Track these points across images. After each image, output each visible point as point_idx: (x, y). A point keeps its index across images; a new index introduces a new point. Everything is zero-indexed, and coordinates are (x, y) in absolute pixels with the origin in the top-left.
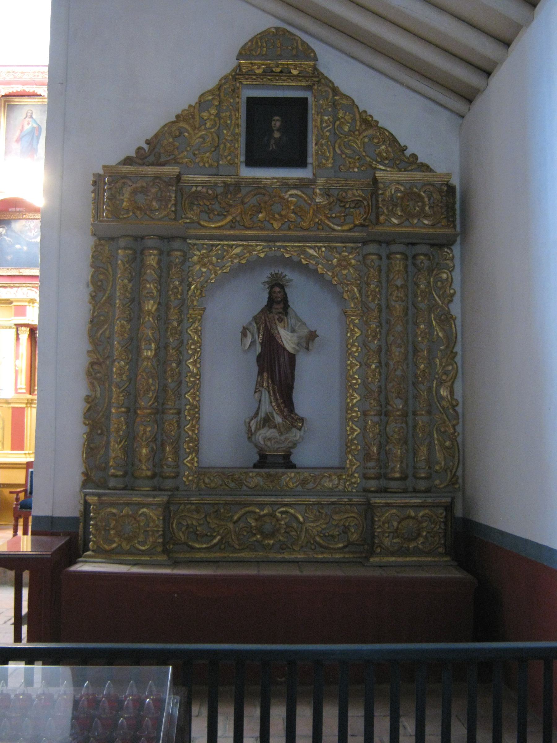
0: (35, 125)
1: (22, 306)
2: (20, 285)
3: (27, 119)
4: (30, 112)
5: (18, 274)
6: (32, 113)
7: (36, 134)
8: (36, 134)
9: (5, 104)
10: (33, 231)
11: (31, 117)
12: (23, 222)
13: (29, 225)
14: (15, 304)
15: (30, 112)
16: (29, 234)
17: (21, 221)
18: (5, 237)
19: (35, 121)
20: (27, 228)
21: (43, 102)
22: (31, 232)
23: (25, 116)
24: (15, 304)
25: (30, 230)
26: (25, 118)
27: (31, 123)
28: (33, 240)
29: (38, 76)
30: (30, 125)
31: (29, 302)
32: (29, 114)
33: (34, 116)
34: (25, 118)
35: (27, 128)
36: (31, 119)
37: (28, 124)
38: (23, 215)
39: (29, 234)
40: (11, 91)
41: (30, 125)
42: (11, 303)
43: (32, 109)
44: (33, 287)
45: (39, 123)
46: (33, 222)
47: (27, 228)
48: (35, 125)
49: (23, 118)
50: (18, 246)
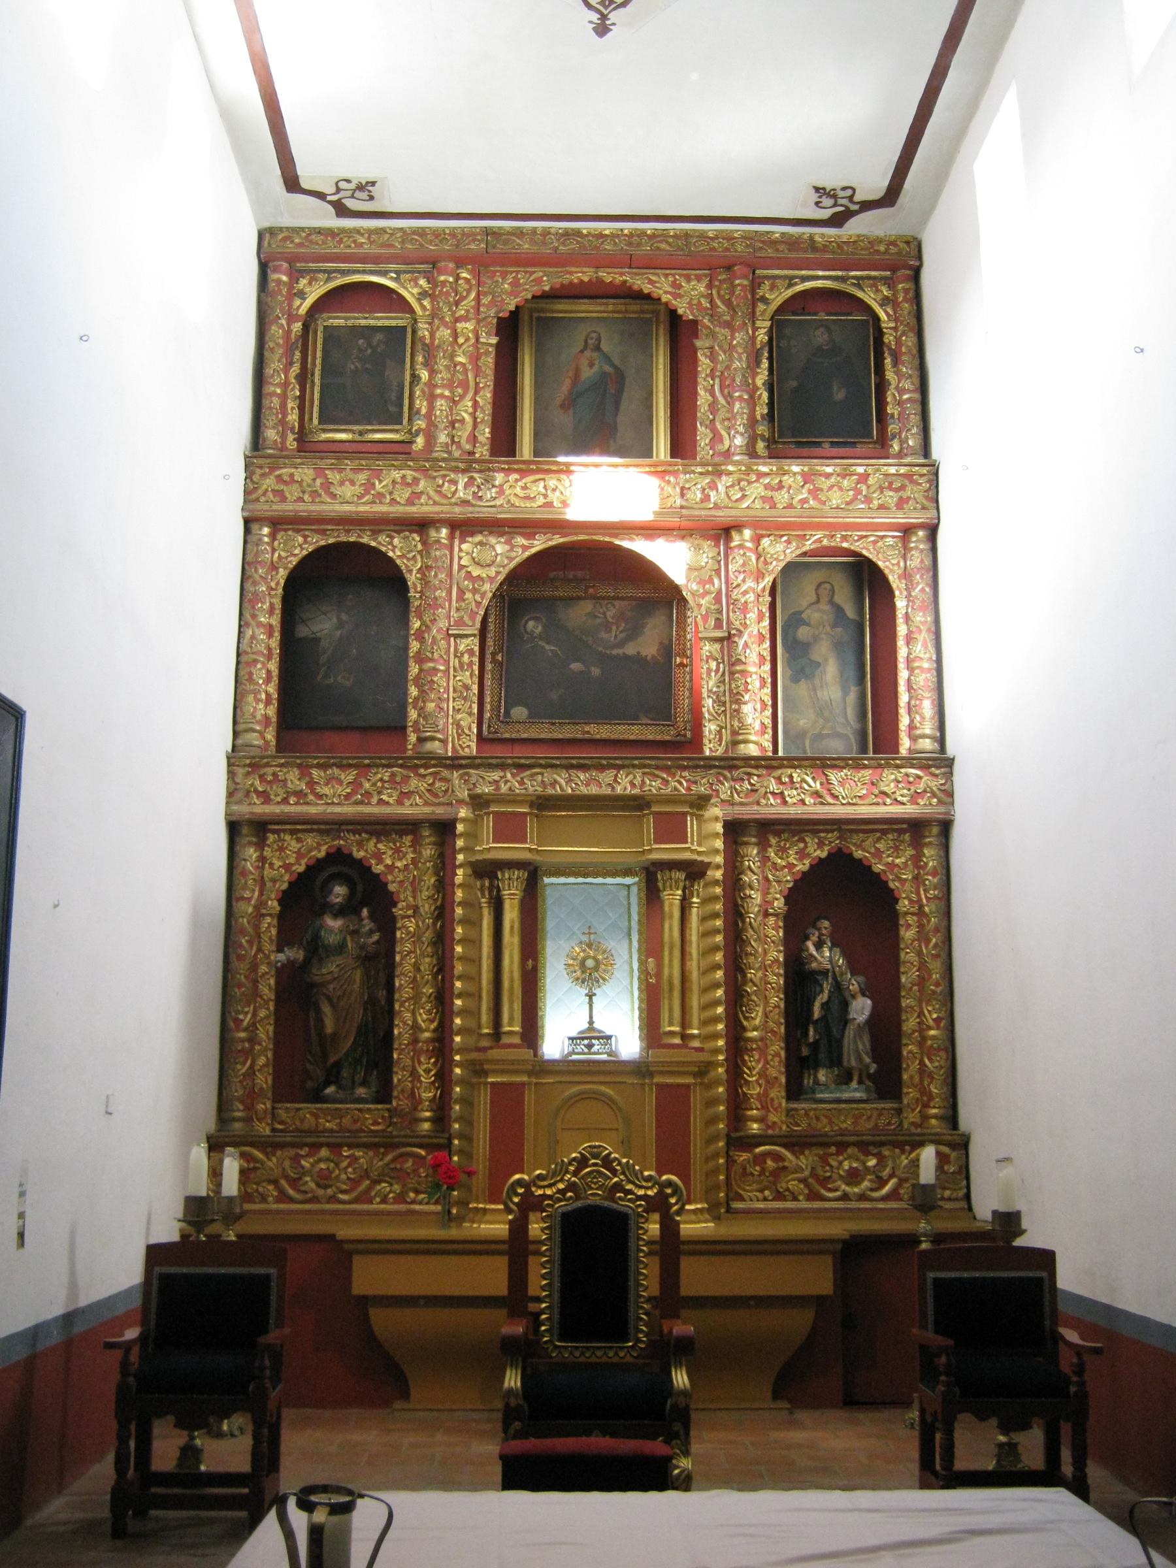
0: (608, 369)
1: (678, 813)
2: (627, 762)
3: (588, 353)
4: (594, 335)
5: (580, 736)
6: (599, 340)
7: (612, 390)
8: (612, 390)
9: (531, 317)
10: (614, 628)
11: (597, 348)
12: (587, 606)
13: (604, 613)
14: (655, 809)
15: (594, 335)
16: (603, 635)
17: (582, 603)
18: (541, 643)
19: (607, 358)
20: (598, 621)
21: (626, 312)
22: (609, 631)
23: (582, 347)
24: (655, 809)
25: (607, 626)
26: (582, 351)
27: (597, 362)
28: (615, 652)
29: (639, 245)
30: (596, 368)
31: (692, 805)
32: (590, 342)
33: (604, 346)
34: (582, 351)
35: (587, 373)
36: (595, 354)
37: (591, 365)
38: (587, 588)
39: (603, 635)
40: (566, 282)
41: (596, 368)
42: (648, 805)
43: (598, 330)
44: (657, 767)
45: (617, 362)
46: (614, 606)
47: (598, 621)
48: (608, 369)
49: (576, 350)
50: (576, 666)
